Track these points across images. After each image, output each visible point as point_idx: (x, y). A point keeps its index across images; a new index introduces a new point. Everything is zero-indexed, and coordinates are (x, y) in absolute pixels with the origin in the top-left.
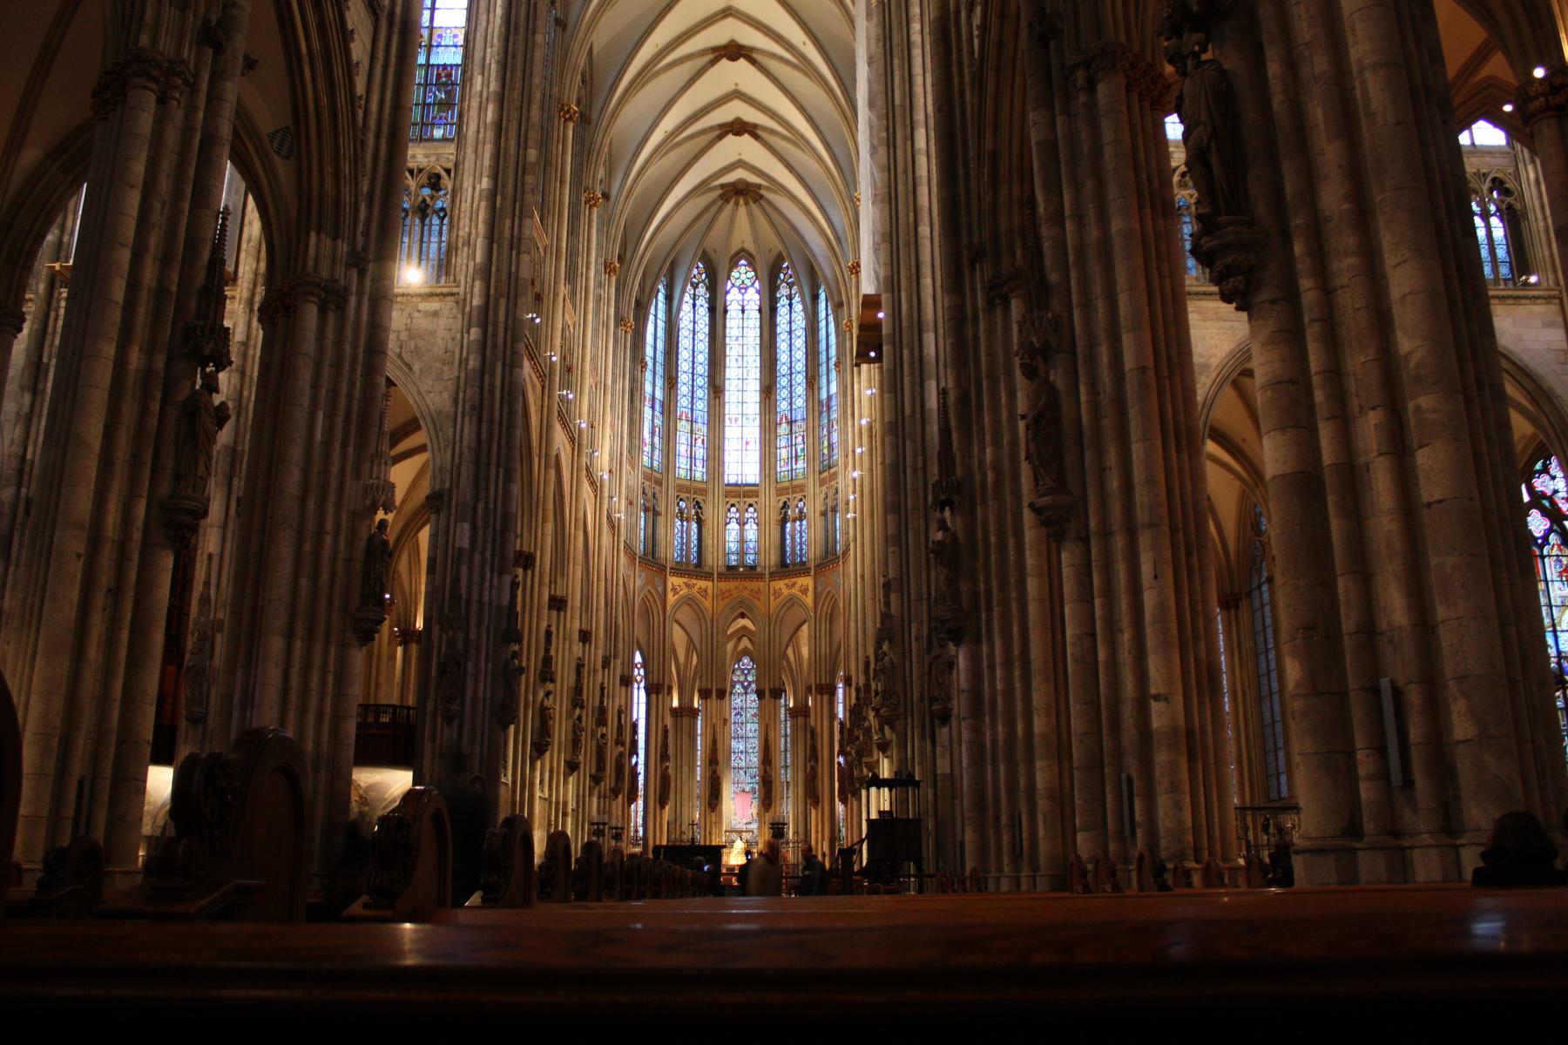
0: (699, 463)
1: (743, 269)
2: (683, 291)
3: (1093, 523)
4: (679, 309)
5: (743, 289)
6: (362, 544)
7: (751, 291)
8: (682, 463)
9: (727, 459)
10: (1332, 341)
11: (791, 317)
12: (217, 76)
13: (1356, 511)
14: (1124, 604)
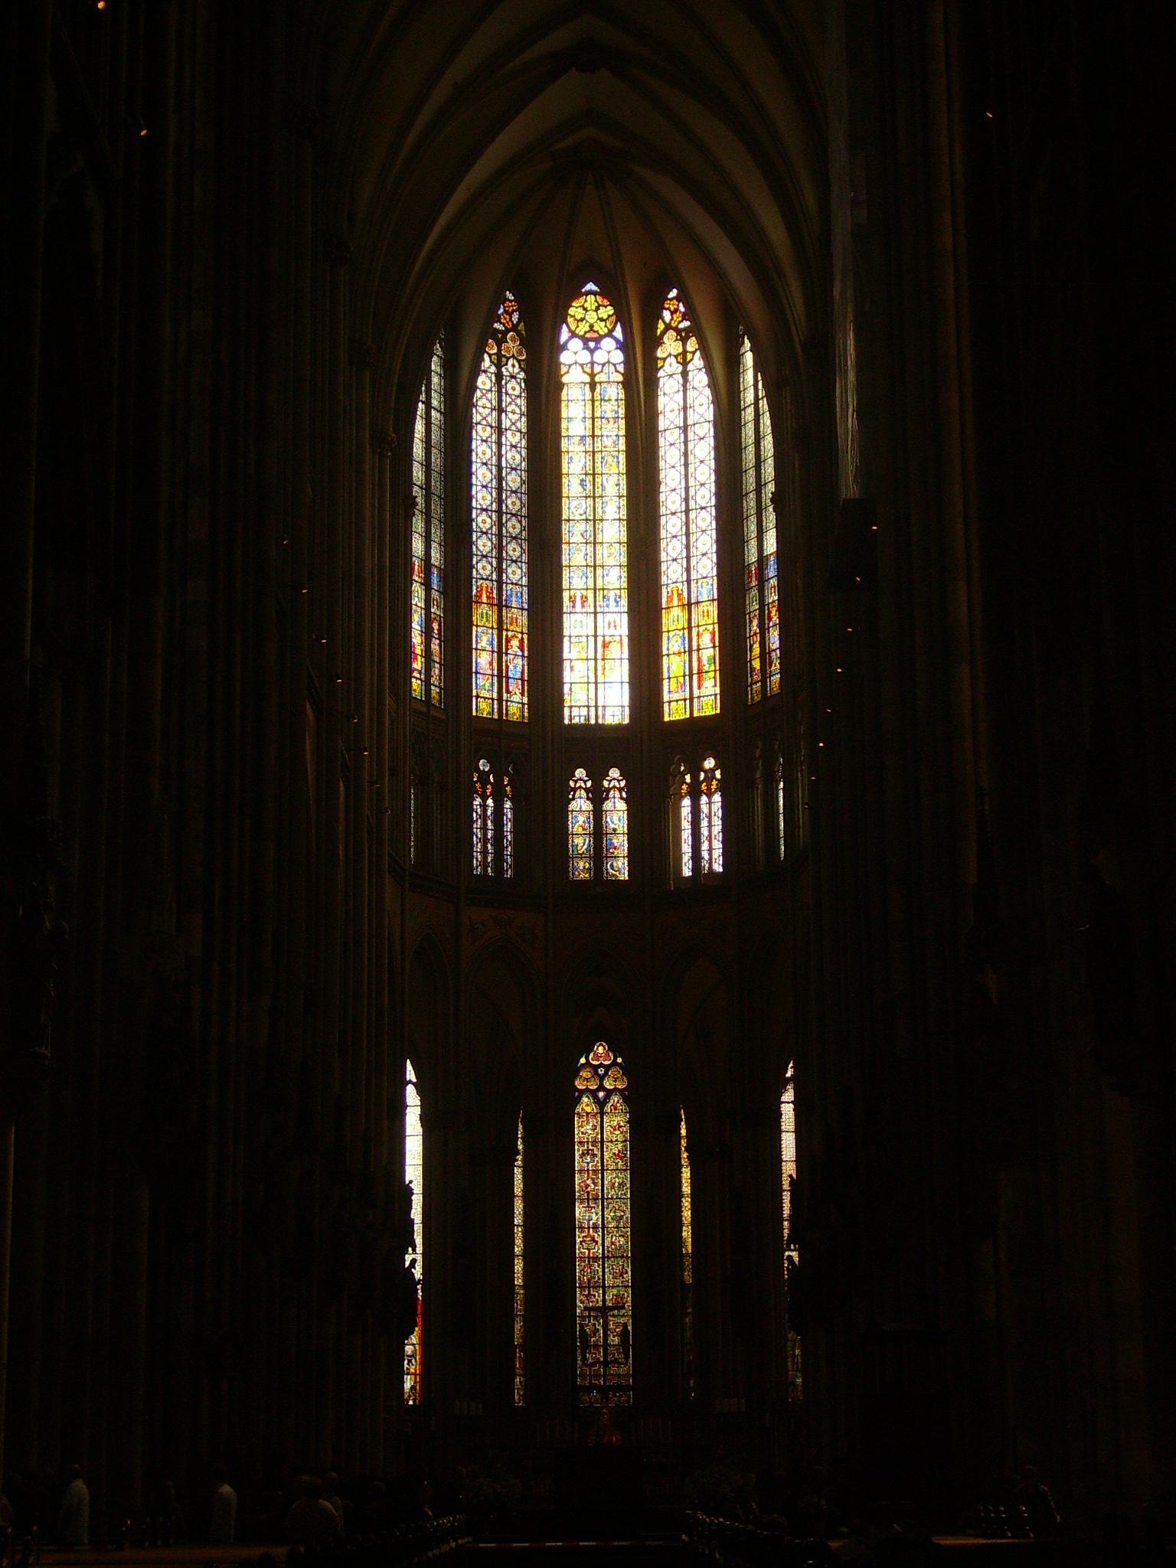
0: (515, 687)
1: (591, 301)
4: (473, 388)
5: (591, 341)
7: (608, 344)
8: (483, 686)
9: (567, 677)
11: (685, 397)
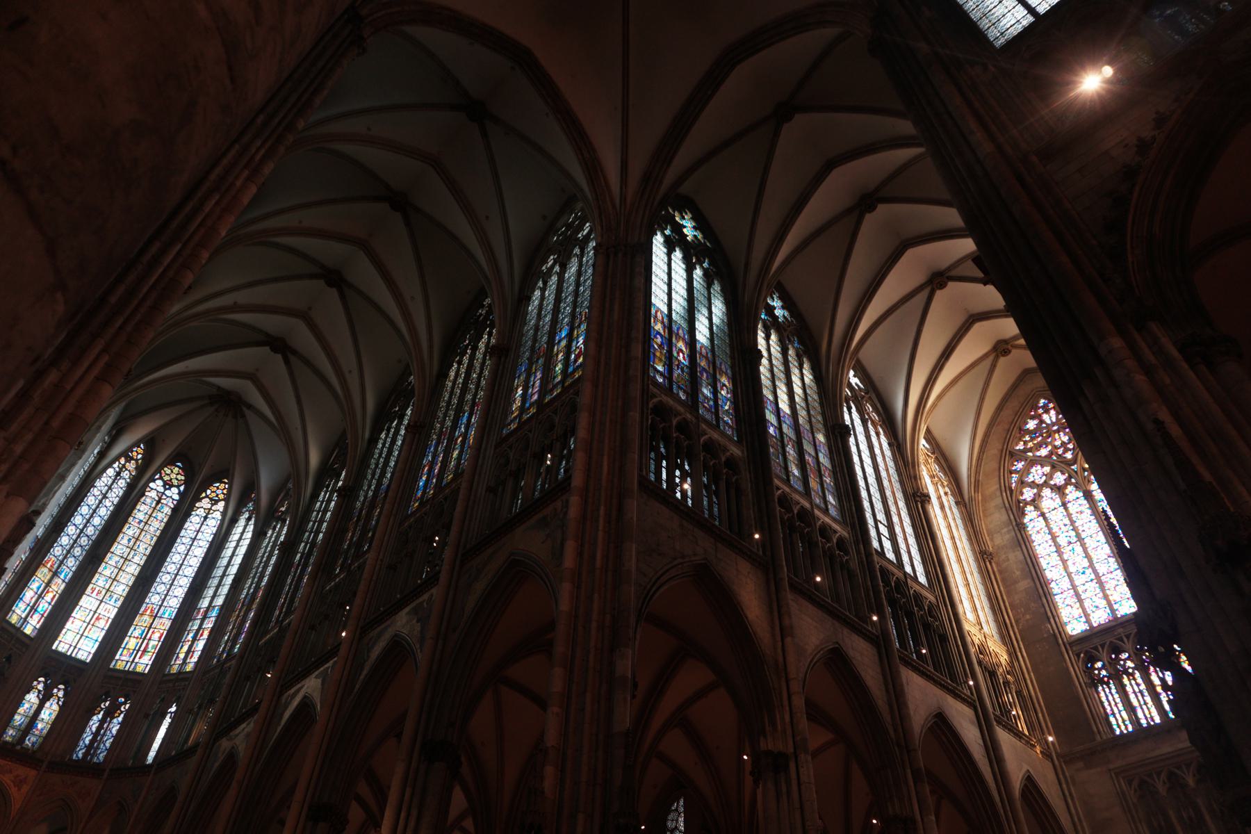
0: (36, 617)
2: (117, 459)
5: (168, 485)
7: (175, 490)
9: (68, 625)
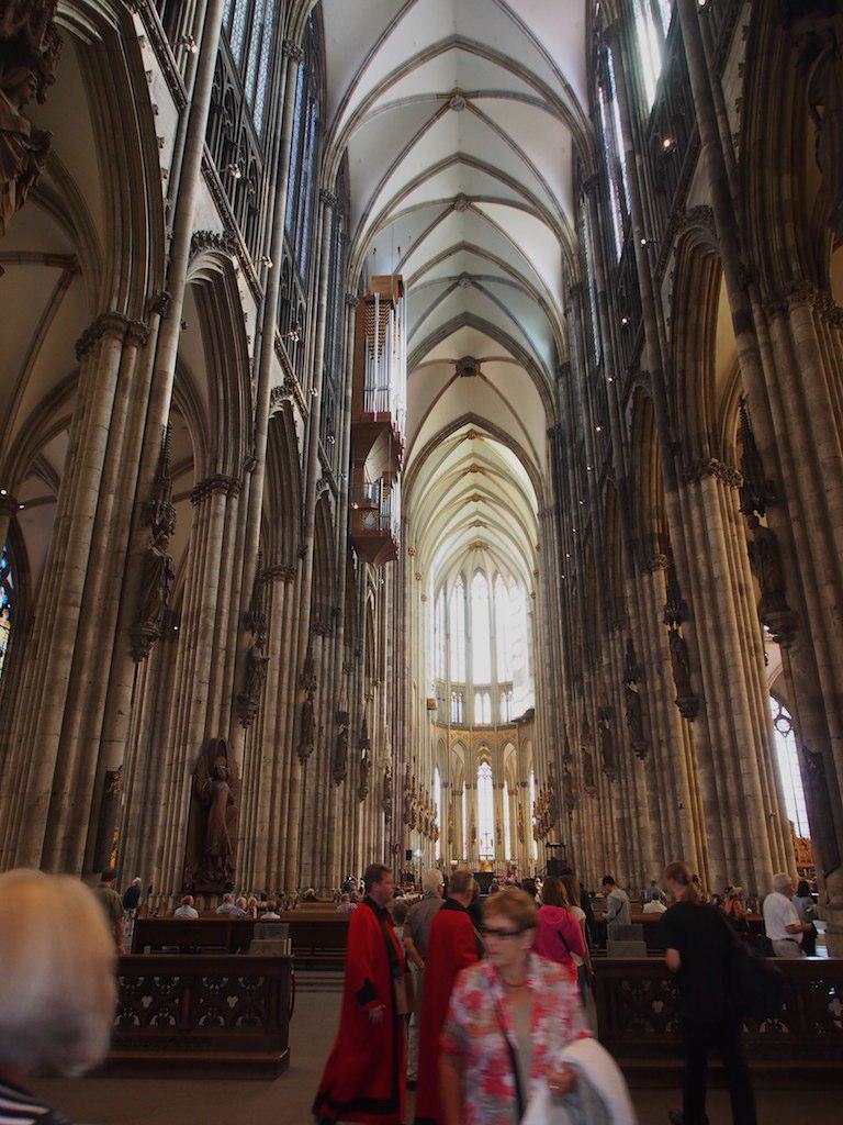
3: (601, 795)
6: (383, 778)
10: (627, 792)
12: (360, 664)
13: (631, 827)
14: (608, 818)
